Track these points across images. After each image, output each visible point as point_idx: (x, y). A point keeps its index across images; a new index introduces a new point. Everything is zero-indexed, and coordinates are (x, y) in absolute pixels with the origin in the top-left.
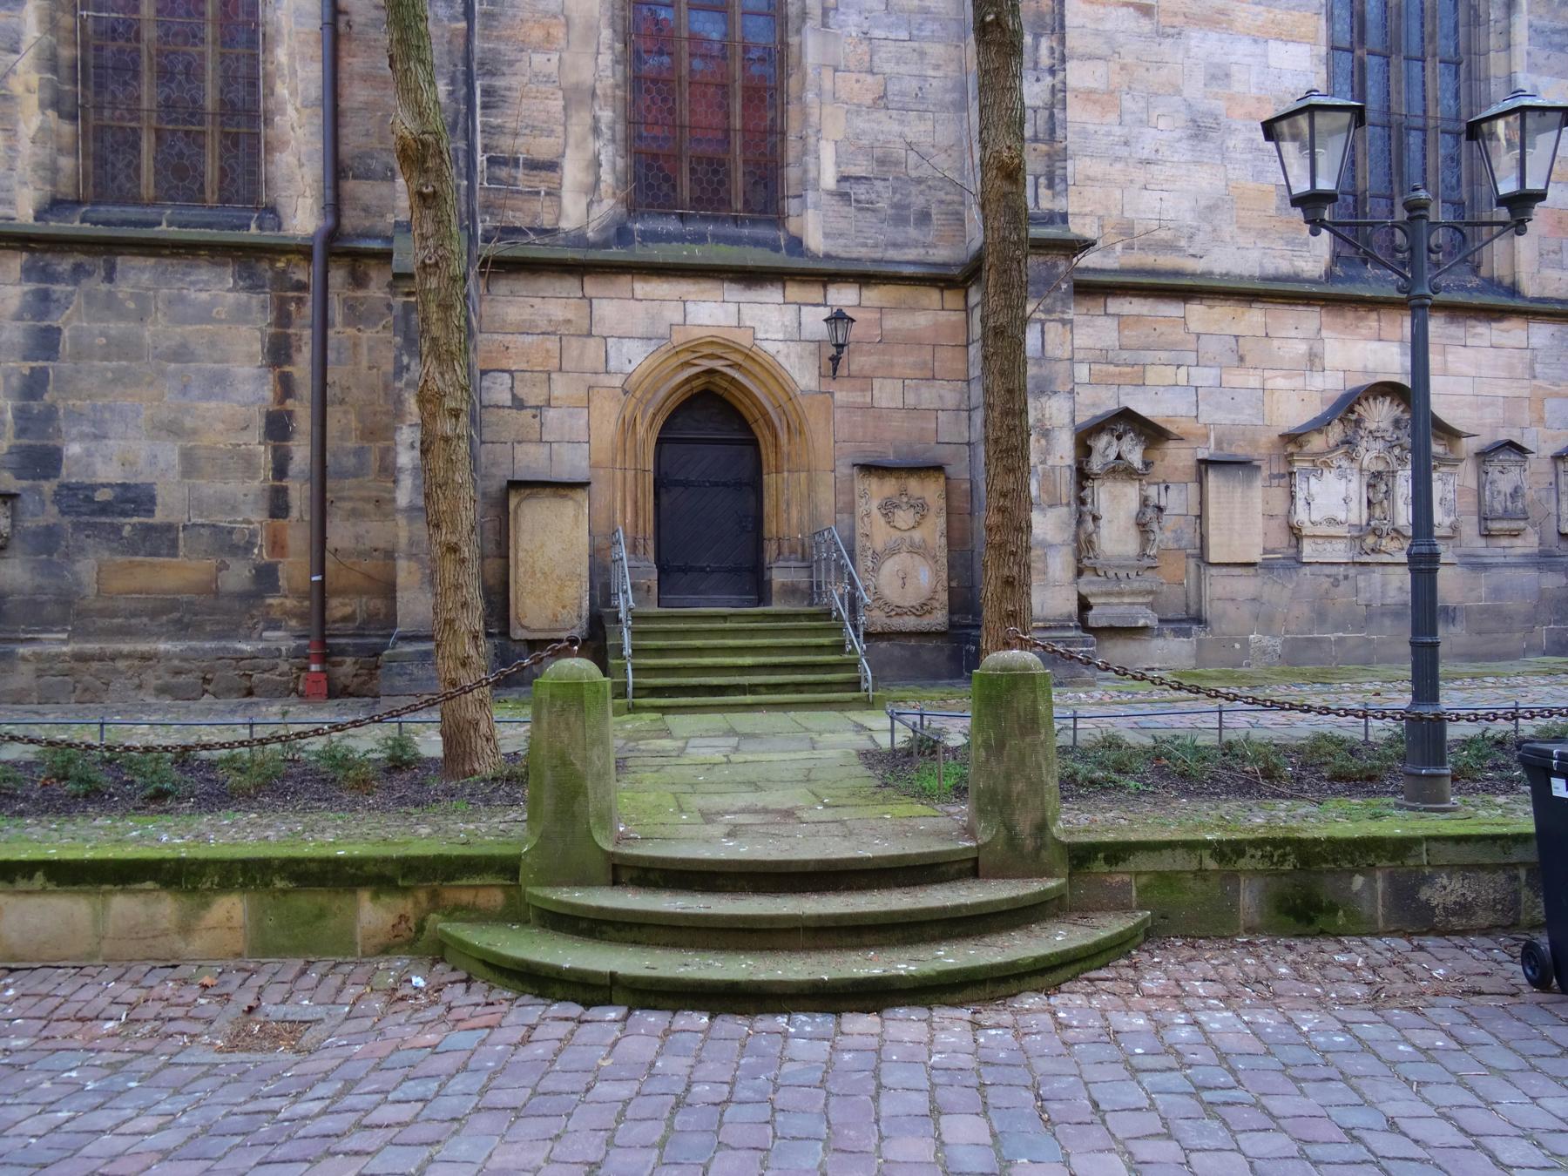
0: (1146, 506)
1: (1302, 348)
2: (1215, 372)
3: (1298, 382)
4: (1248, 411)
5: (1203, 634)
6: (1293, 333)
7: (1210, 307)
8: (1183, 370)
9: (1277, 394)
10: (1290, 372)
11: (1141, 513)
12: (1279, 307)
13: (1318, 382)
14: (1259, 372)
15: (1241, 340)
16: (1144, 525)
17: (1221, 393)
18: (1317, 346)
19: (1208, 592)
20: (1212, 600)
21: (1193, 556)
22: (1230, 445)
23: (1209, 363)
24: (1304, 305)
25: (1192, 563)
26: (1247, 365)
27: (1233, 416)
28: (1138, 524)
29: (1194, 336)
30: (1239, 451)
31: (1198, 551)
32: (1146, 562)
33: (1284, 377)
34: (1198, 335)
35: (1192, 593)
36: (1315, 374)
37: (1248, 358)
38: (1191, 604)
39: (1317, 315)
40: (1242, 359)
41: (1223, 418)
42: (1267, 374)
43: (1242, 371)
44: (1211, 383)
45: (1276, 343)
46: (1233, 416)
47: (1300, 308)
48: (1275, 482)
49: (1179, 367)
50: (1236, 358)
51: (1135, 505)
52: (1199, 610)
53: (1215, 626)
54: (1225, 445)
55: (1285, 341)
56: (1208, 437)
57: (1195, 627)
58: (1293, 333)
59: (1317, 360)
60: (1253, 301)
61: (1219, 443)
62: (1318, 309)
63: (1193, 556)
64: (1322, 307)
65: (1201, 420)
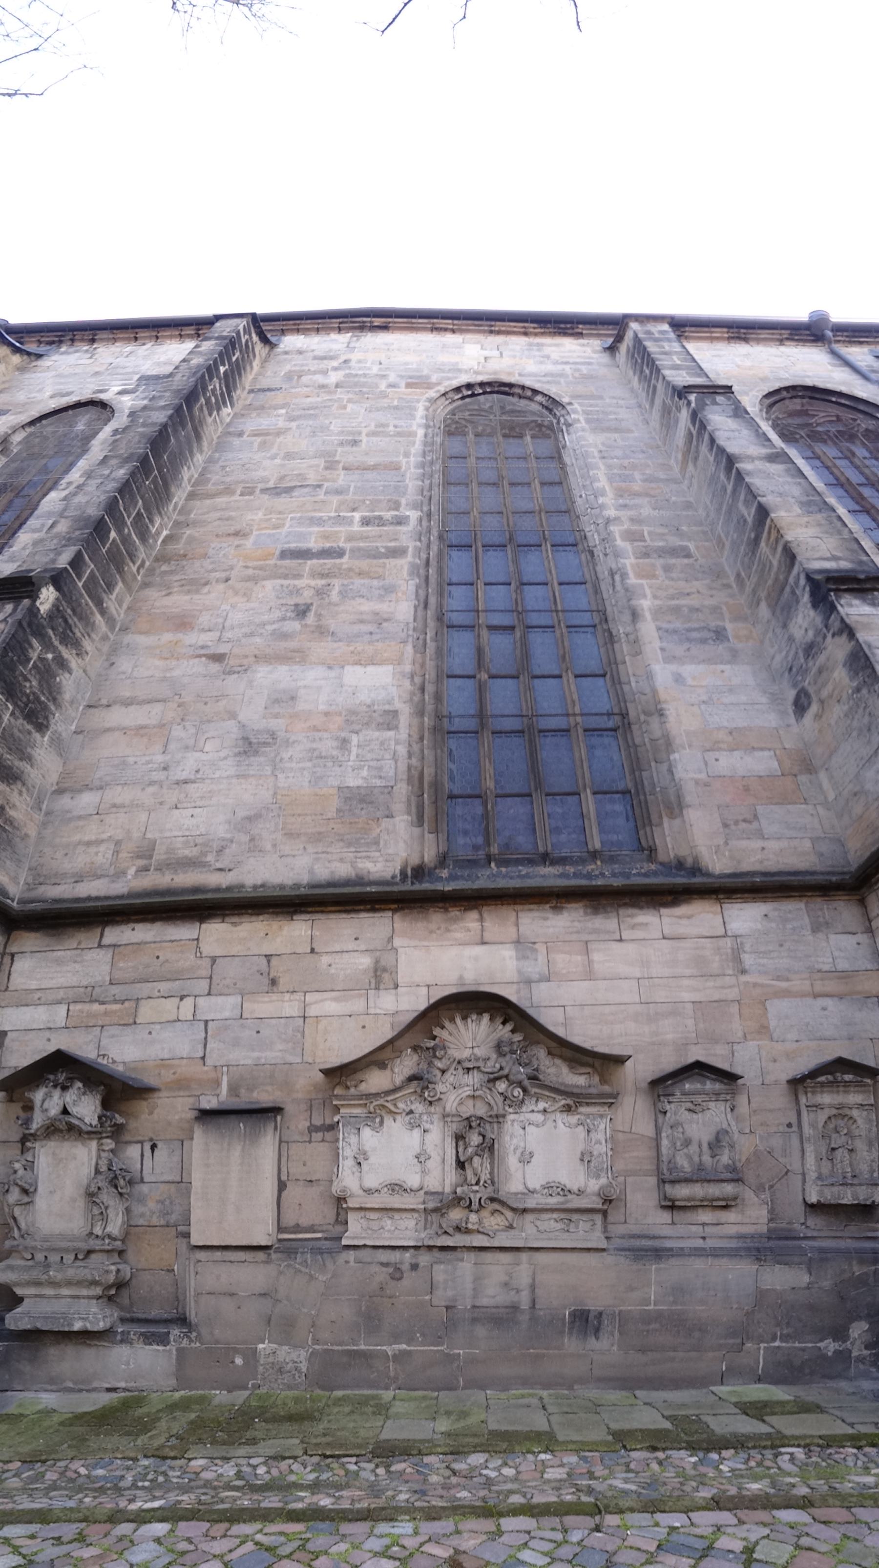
1: (366, 961)
2: (235, 1000)
3: (358, 1005)
4: (280, 1046)
6: (352, 945)
7: (234, 924)
9: (324, 1023)
10: (347, 990)
12: (332, 916)
15: (274, 961)
17: (242, 1026)
18: (387, 960)
24: (368, 911)
27: (256, 1054)
29: (208, 960)
33: (335, 999)
34: (214, 960)
39: (388, 921)
40: (274, 982)
41: (243, 1057)
43: (274, 997)
44: (227, 1014)
45: (325, 960)
46: (256, 1054)
50: (266, 981)
55: (337, 957)
56: (218, 1083)
58: (352, 945)
59: (386, 976)
60: (295, 912)
65: (208, 1061)
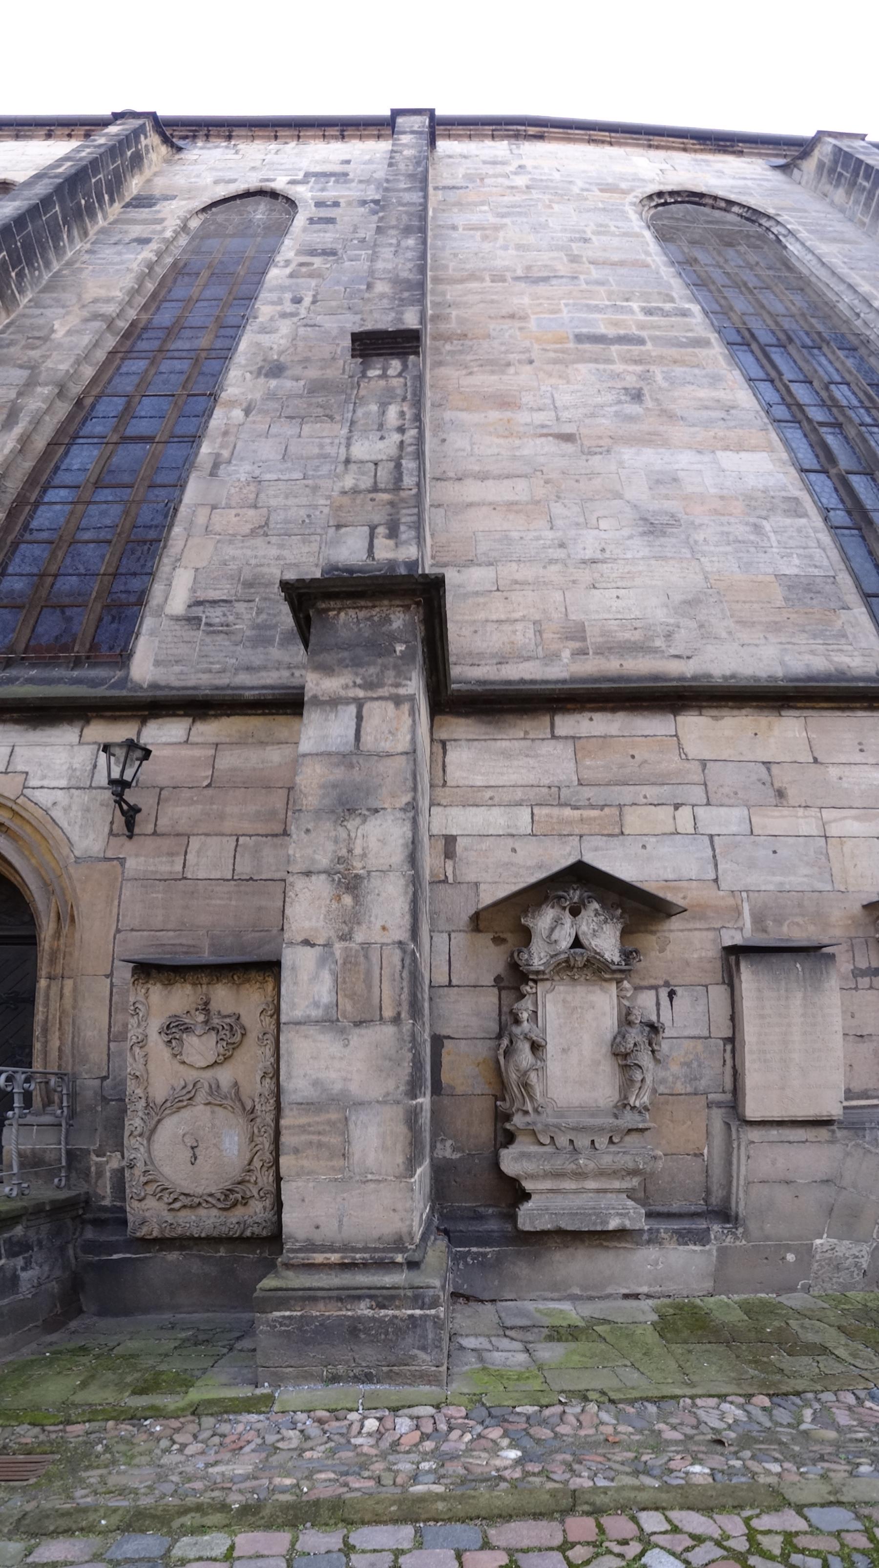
0: (630, 1023)
5: (729, 1239)
11: (621, 1035)
16: (626, 1056)
19: (743, 1170)
20: (748, 1183)
21: (719, 1105)
25: (718, 1116)
28: (616, 1055)
31: (728, 1097)
32: (629, 1119)
35: (717, 1172)
38: (715, 1188)
51: (609, 1023)
52: (727, 1199)
53: (752, 1225)
57: (716, 1228)
63: (719, 1105)
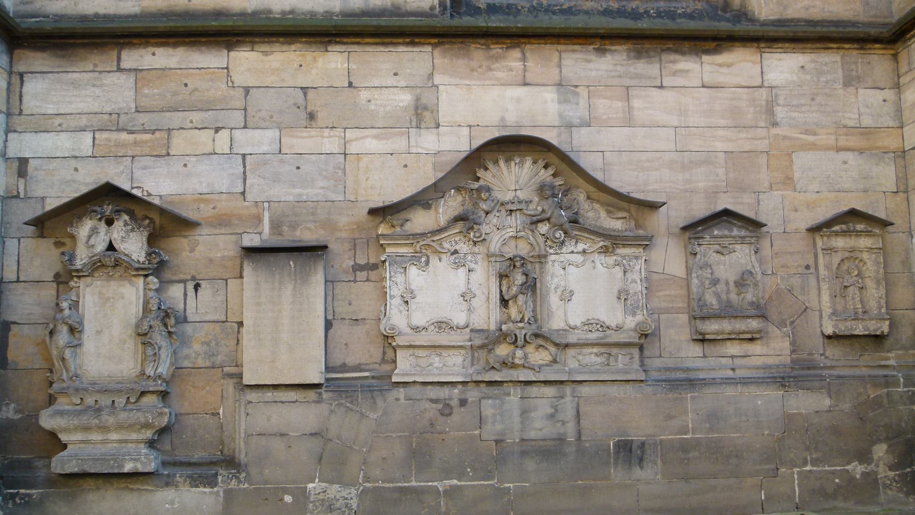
1: (406, 98)
2: (273, 134)
3: (399, 144)
6: (391, 81)
8: (224, 135)
9: (365, 159)
10: (388, 128)
13: (428, 141)
14: (338, 132)
15: (311, 94)
17: (282, 161)
18: (427, 98)
22: (293, 227)
23: (263, 124)
24: (407, 44)
26: (320, 123)
30: (307, 236)
33: (376, 137)
36: (423, 131)
37: (320, 115)
40: (312, 116)
41: (284, 193)
42: (350, 134)
43: (313, 132)
44: (265, 148)
45: (364, 95)
47: (402, 49)
48: (362, 275)
49: (217, 130)
50: (303, 115)
54: (285, 228)
55: (378, 91)
56: (259, 219)
58: (391, 81)
59: (427, 114)
61: (276, 226)
62: (429, 49)
64: (435, 46)
65: (249, 197)
